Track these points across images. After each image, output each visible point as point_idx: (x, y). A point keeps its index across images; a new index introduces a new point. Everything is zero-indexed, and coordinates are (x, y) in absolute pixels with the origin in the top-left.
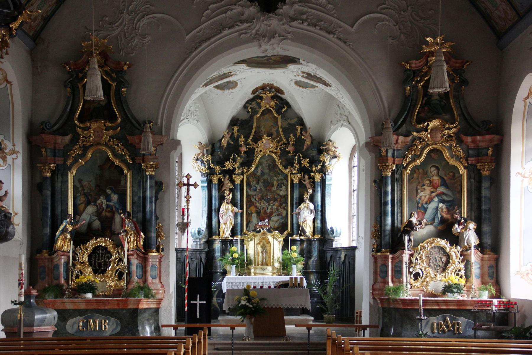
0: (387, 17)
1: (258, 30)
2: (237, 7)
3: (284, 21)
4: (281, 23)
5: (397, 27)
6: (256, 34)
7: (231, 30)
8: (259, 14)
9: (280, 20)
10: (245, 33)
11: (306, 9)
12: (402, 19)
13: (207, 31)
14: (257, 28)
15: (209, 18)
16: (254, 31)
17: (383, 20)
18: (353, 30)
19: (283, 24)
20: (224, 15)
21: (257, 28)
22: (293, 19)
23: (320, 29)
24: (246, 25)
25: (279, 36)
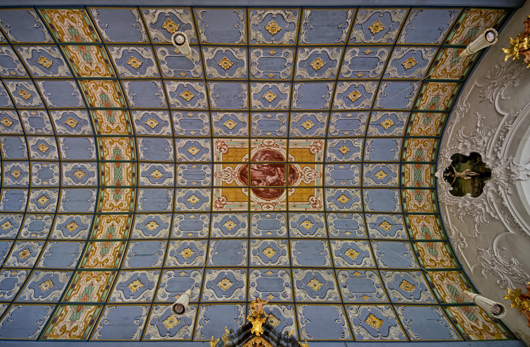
0: (499, 93)
1: (505, 181)
2: (488, 194)
3: (497, 163)
4: (499, 165)
5: (505, 85)
6: (508, 182)
7: (505, 199)
8: (492, 180)
9: (497, 165)
10: (508, 190)
11: (491, 150)
12: (500, 84)
13: (506, 216)
14: (503, 182)
15: (496, 214)
16: (506, 184)
17: (500, 96)
18: (506, 115)
19: (501, 164)
20: (494, 204)
21: (503, 182)
22: (497, 158)
23: (505, 137)
24: (500, 188)
25: (509, 166)
